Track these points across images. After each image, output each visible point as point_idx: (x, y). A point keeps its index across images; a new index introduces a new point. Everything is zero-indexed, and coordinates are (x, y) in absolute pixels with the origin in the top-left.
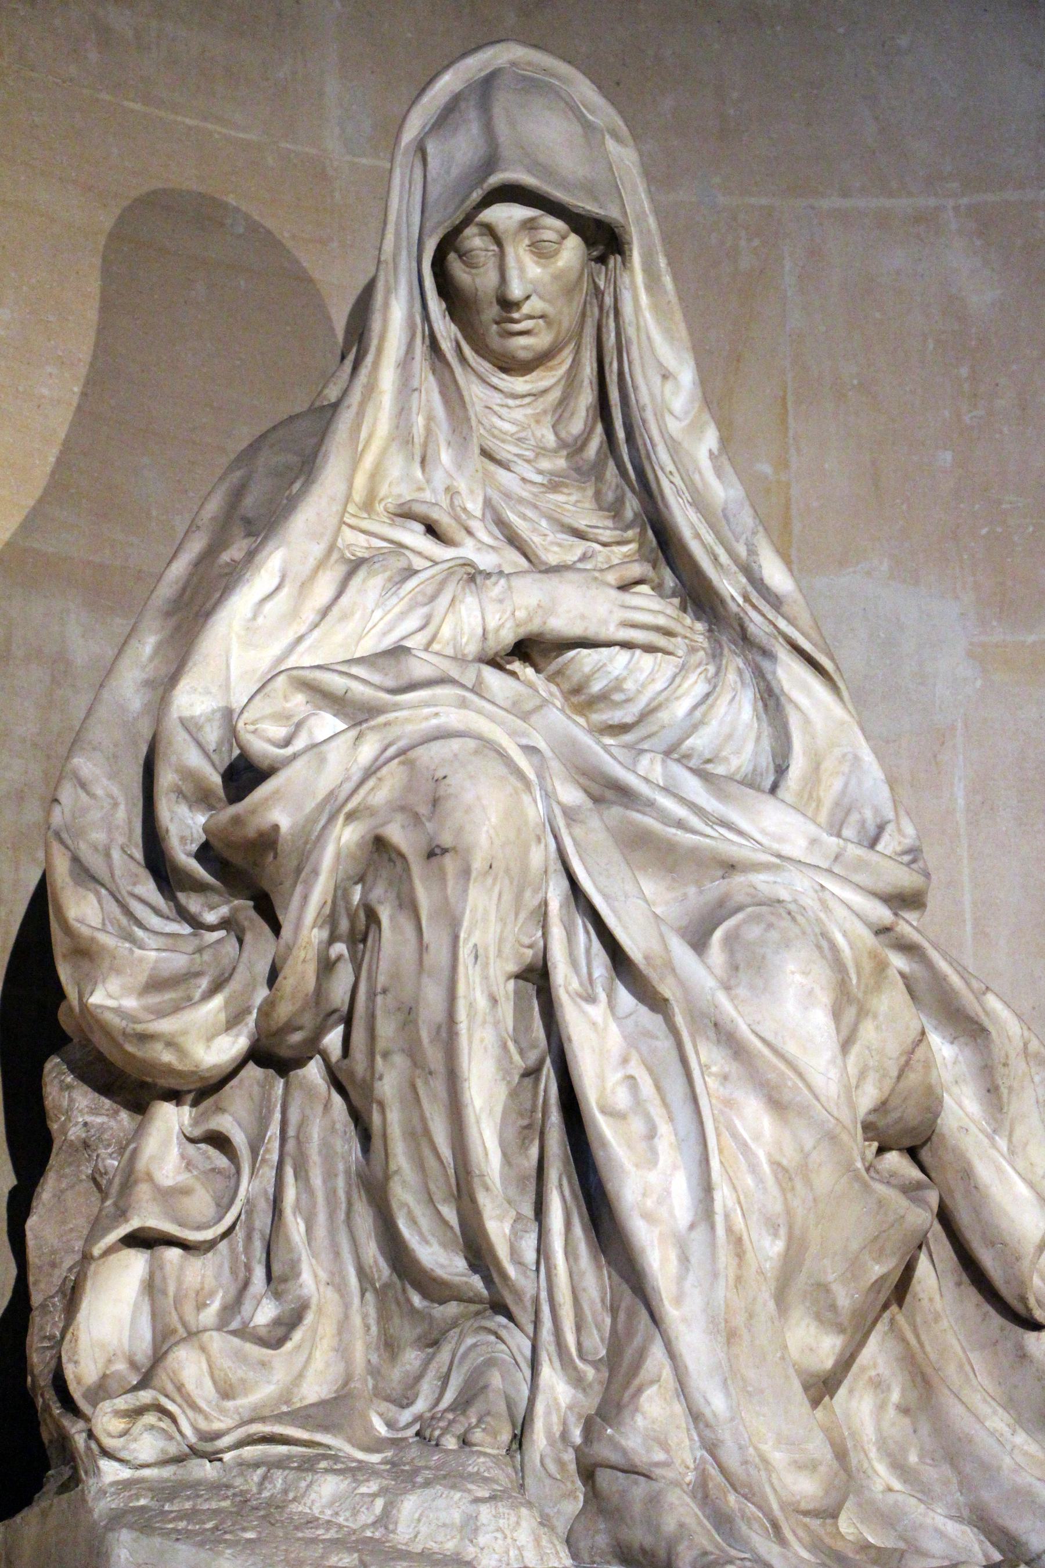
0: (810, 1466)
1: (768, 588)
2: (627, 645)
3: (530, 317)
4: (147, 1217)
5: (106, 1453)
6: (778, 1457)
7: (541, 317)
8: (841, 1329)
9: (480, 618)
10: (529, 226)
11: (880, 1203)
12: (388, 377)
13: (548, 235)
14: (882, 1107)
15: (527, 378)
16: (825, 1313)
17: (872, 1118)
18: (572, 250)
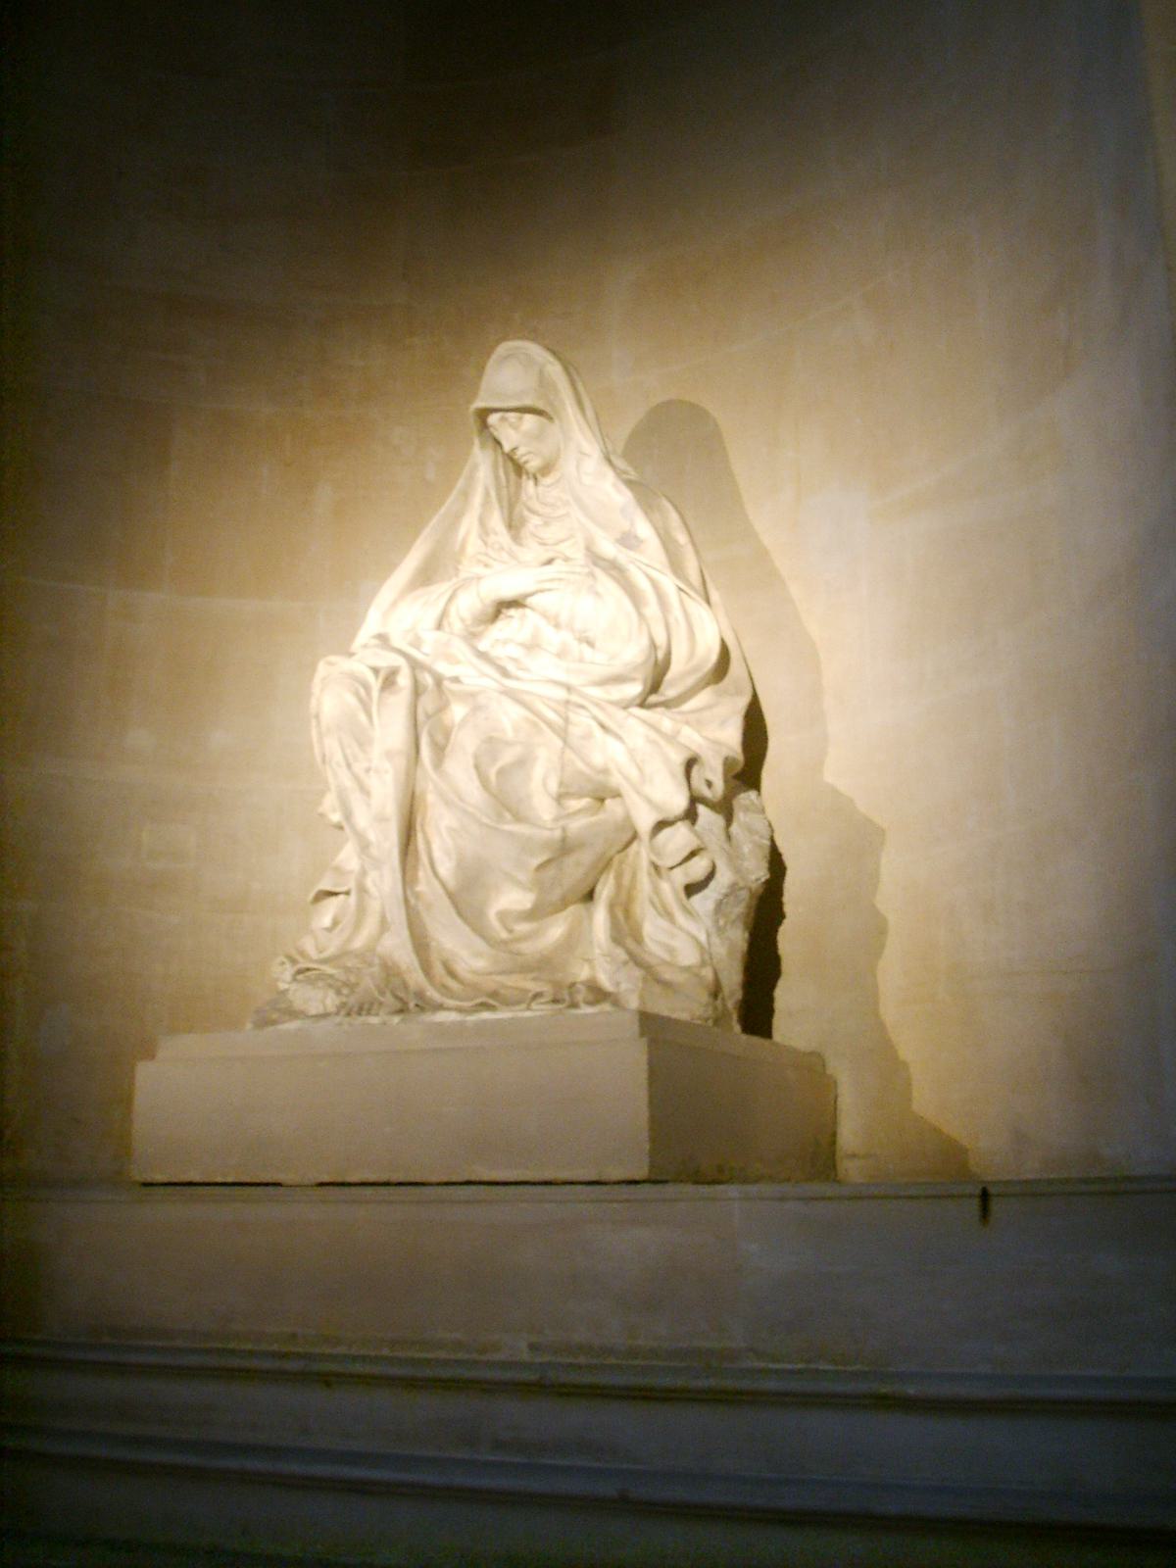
0: (478, 955)
1: (636, 537)
2: (542, 591)
3: (524, 455)
4: (326, 885)
5: (277, 980)
6: (464, 954)
7: (530, 453)
8: (531, 890)
9: (469, 603)
10: (503, 419)
11: (511, 834)
12: (477, 499)
13: (513, 420)
14: (561, 784)
15: (552, 475)
16: (519, 884)
17: (563, 790)
18: (530, 420)
